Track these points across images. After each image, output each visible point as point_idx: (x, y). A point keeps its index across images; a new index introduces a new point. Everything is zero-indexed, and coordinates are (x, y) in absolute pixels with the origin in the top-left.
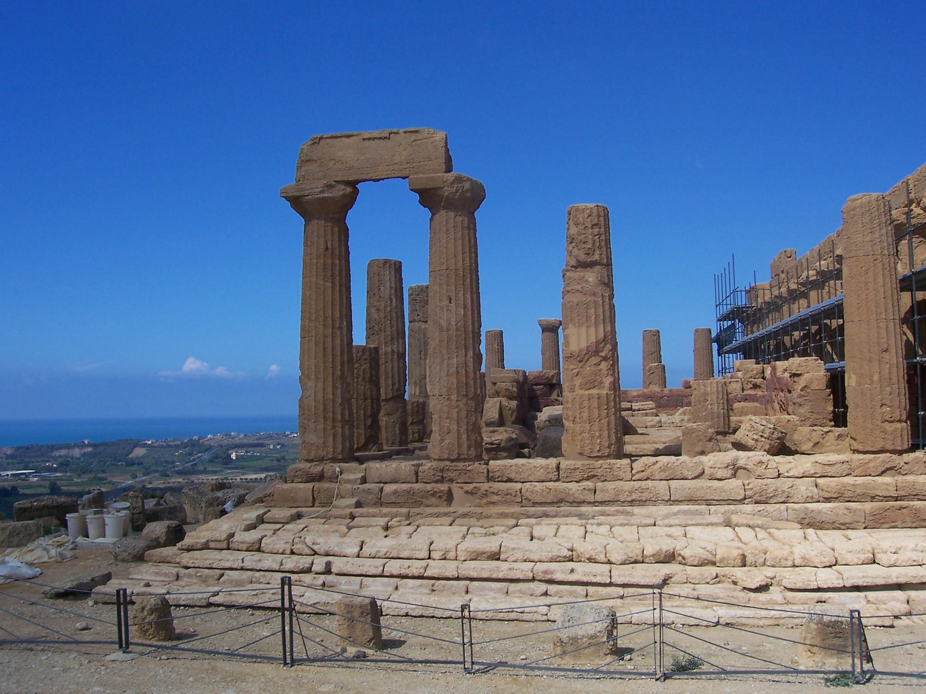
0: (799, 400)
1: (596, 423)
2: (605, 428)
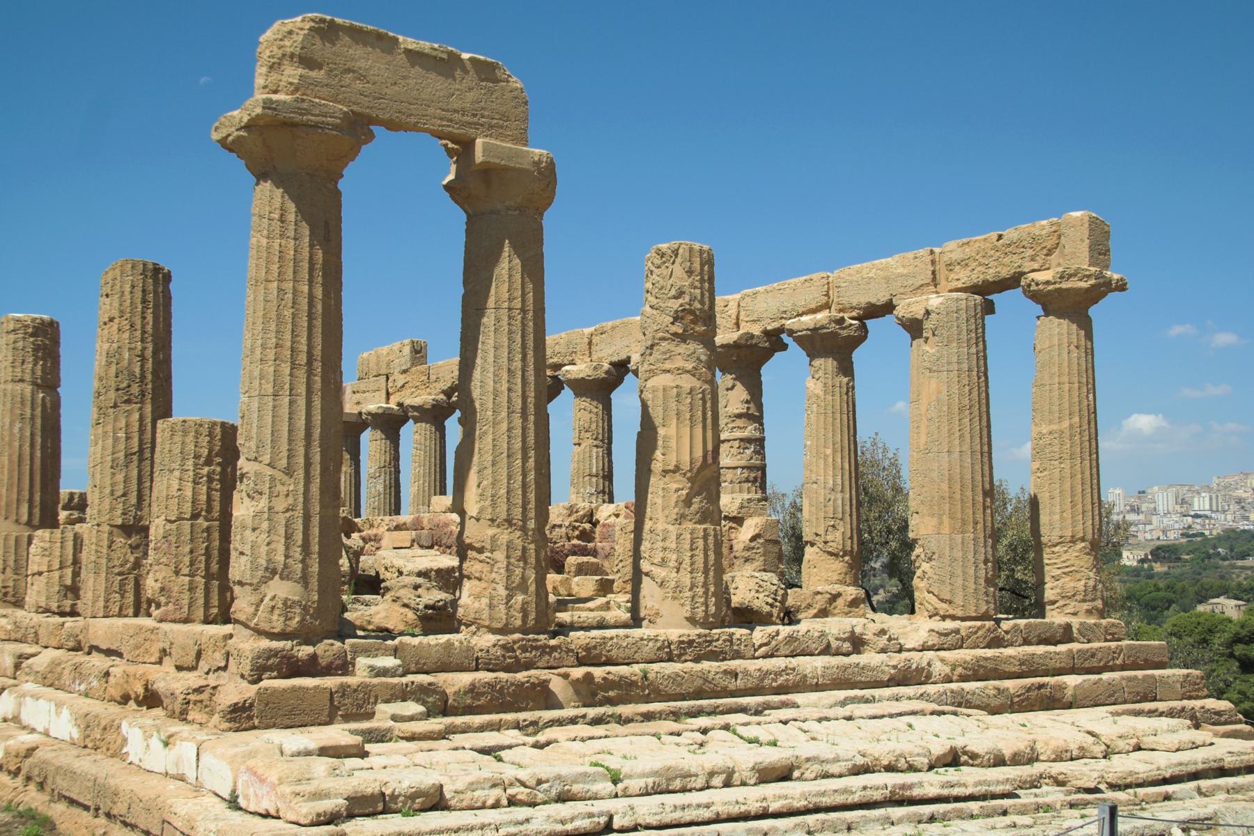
0: (747, 554)
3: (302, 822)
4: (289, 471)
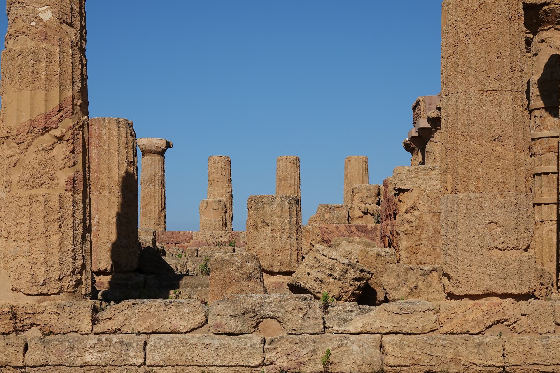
1: (41, 242)
2: (55, 249)
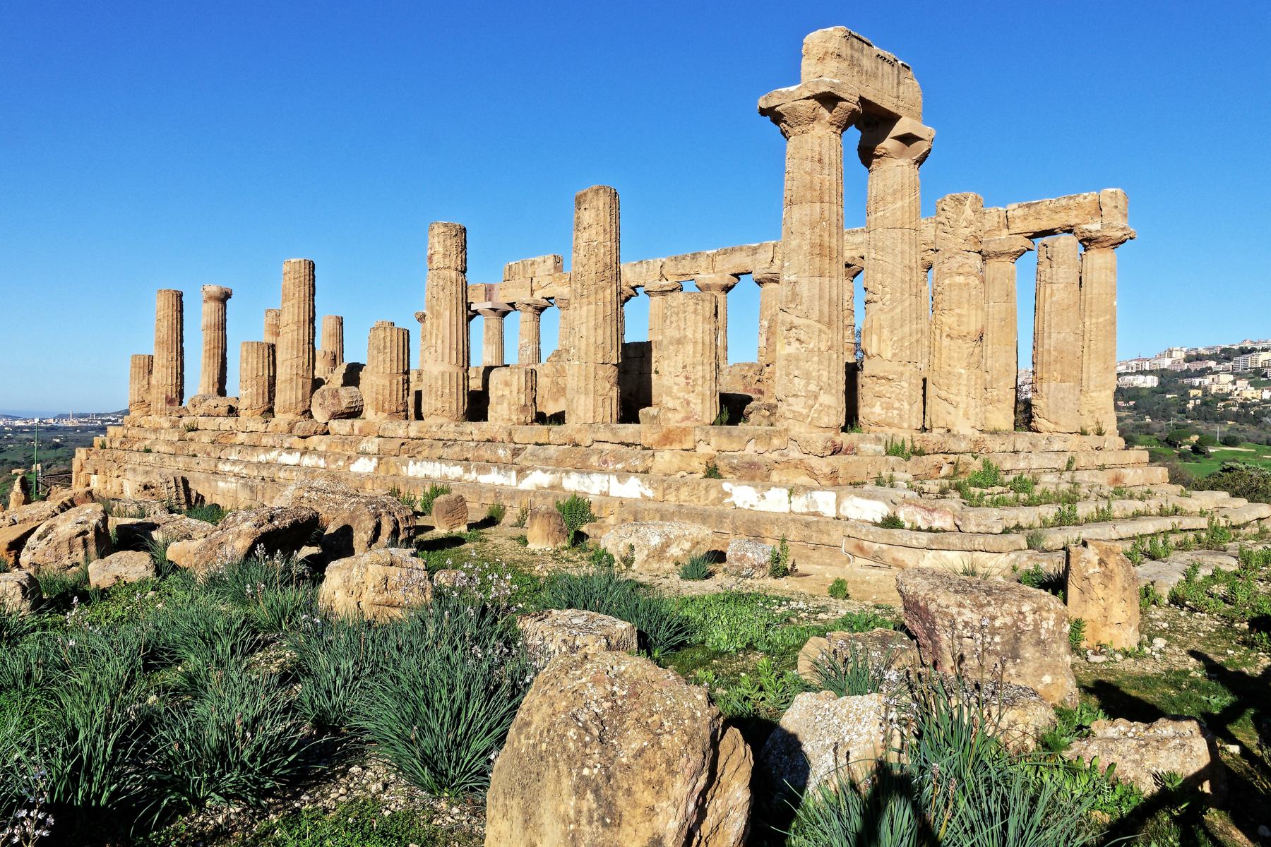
3: (995, 531)
4: (829, 324)
